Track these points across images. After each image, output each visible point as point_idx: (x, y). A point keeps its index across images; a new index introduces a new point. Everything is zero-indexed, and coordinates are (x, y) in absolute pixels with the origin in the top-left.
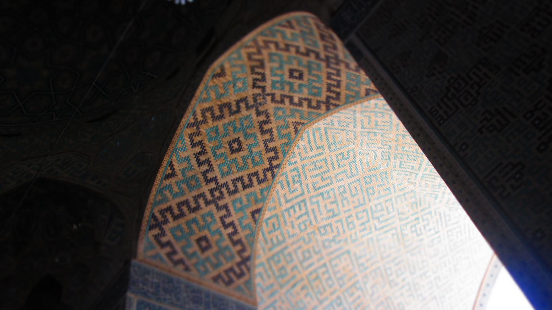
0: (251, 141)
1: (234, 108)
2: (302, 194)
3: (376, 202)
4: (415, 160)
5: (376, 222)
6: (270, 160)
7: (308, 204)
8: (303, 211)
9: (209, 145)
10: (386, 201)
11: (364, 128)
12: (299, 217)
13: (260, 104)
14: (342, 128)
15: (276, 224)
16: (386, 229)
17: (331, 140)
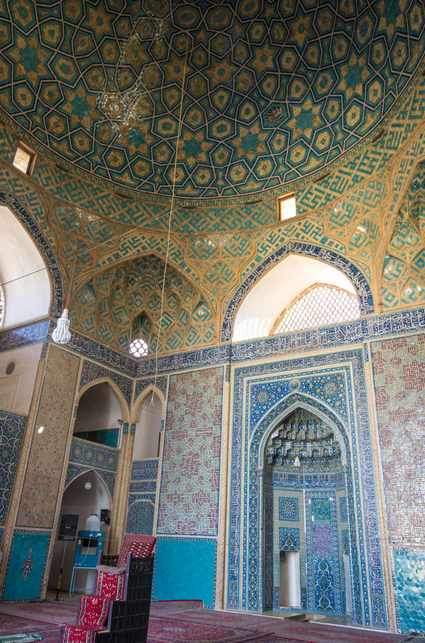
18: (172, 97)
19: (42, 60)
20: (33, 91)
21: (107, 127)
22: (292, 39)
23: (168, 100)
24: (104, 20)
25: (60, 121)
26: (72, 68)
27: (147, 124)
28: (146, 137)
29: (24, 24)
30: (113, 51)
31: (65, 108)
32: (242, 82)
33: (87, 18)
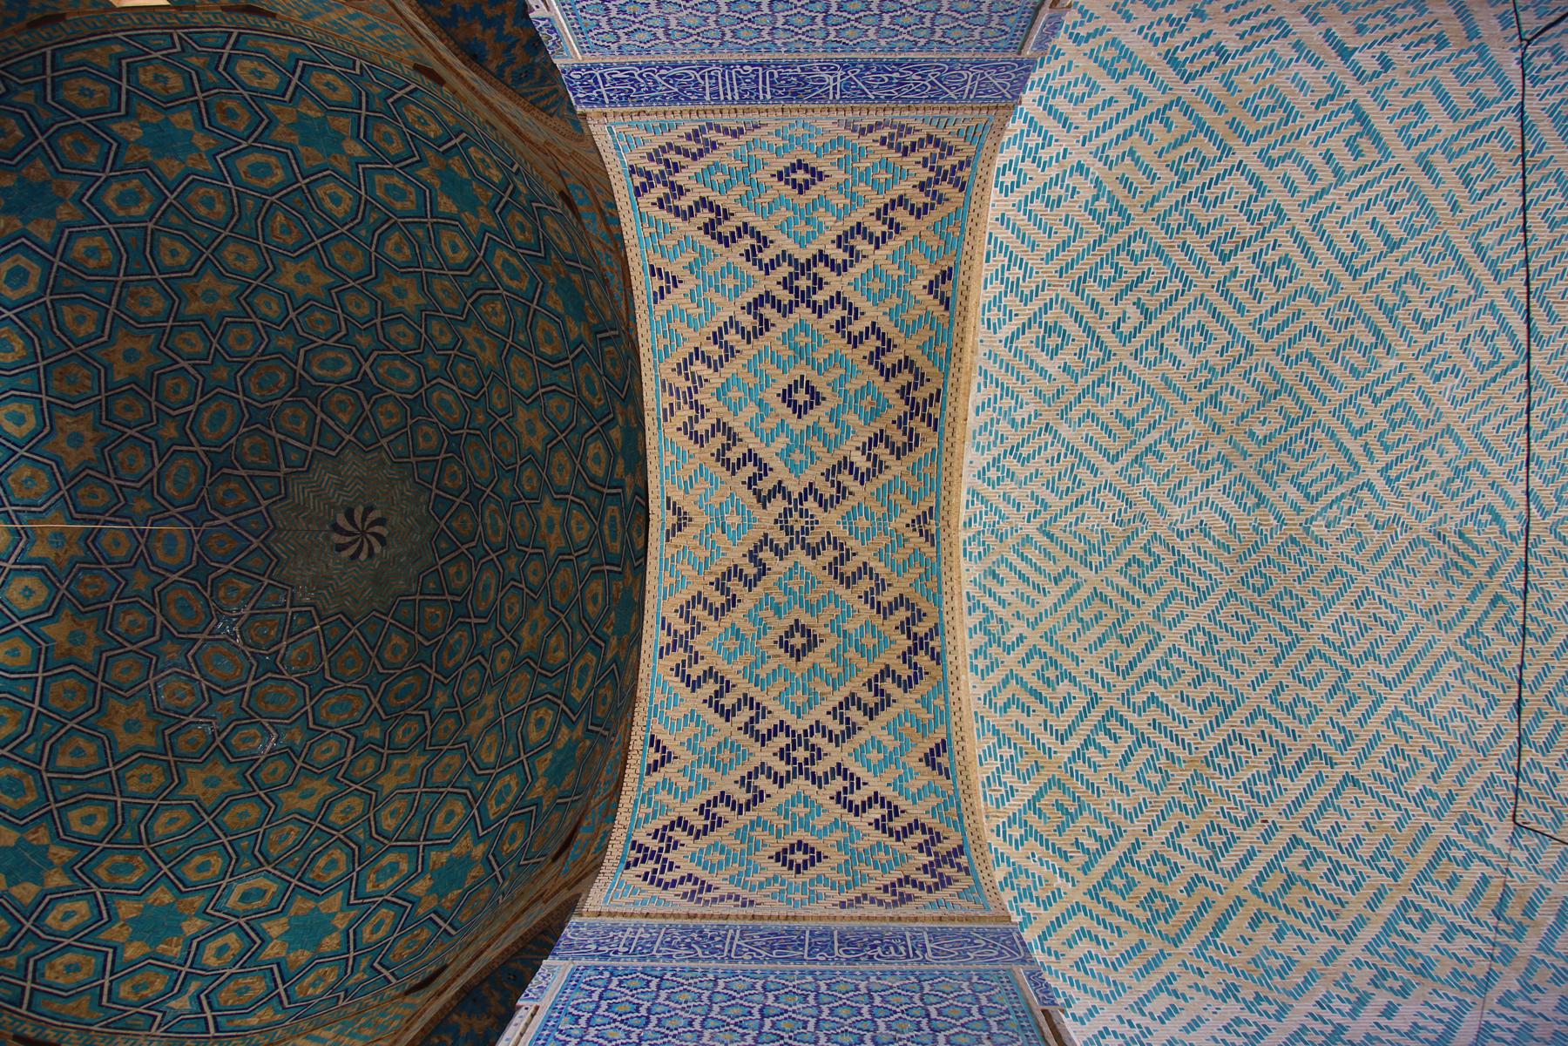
0: (831, 612)
1: (750, 570)
2: (1094, 701)
3: (1328, 620)
4: (1314, 445)
5: (1370, 665)
6: (905, 627)
7: (1132, 717)
8: (1128, 739)
9: (730, 670)
10: (1357, 604)
11: (1116, 457)
12: (1125, 760)
13: (805, 531)
14: (1073, 497)
15: (1067, 801)
16: (1419, 671)
17: (1079, 547)
18: (80, 320)
19: (302, 149)
20: (257, 99)
21: (92, 159)
22: (67, 611)
23: (78, 308)
24: (301, 287)
25: (166, 90)
26: (254, 181)
27: (47, 240)
28: (19, 223)
29: (377, 178)
30: (240, 264)
31: (188, 116)
32: (32, 477)
33: (320, 265)
